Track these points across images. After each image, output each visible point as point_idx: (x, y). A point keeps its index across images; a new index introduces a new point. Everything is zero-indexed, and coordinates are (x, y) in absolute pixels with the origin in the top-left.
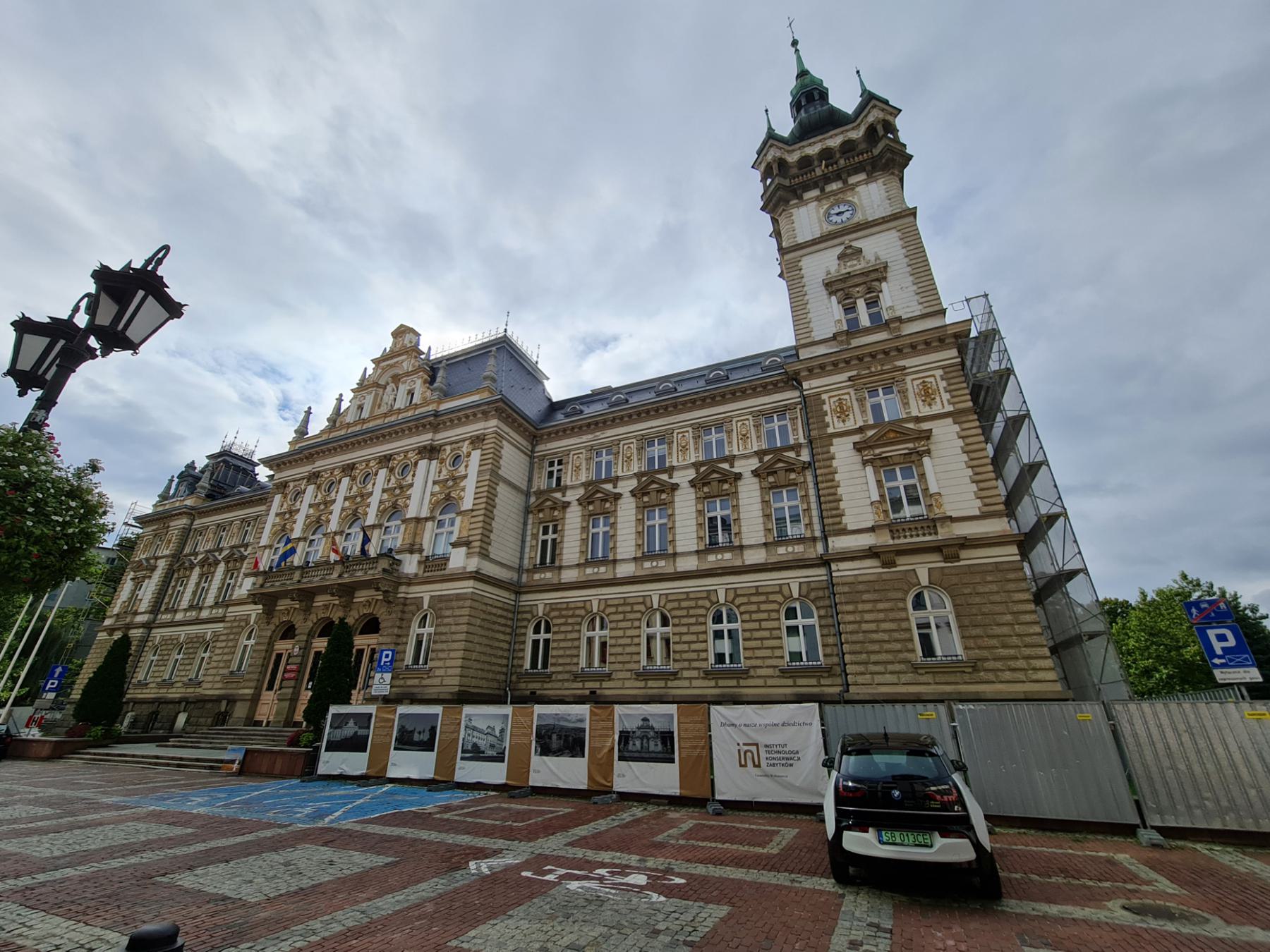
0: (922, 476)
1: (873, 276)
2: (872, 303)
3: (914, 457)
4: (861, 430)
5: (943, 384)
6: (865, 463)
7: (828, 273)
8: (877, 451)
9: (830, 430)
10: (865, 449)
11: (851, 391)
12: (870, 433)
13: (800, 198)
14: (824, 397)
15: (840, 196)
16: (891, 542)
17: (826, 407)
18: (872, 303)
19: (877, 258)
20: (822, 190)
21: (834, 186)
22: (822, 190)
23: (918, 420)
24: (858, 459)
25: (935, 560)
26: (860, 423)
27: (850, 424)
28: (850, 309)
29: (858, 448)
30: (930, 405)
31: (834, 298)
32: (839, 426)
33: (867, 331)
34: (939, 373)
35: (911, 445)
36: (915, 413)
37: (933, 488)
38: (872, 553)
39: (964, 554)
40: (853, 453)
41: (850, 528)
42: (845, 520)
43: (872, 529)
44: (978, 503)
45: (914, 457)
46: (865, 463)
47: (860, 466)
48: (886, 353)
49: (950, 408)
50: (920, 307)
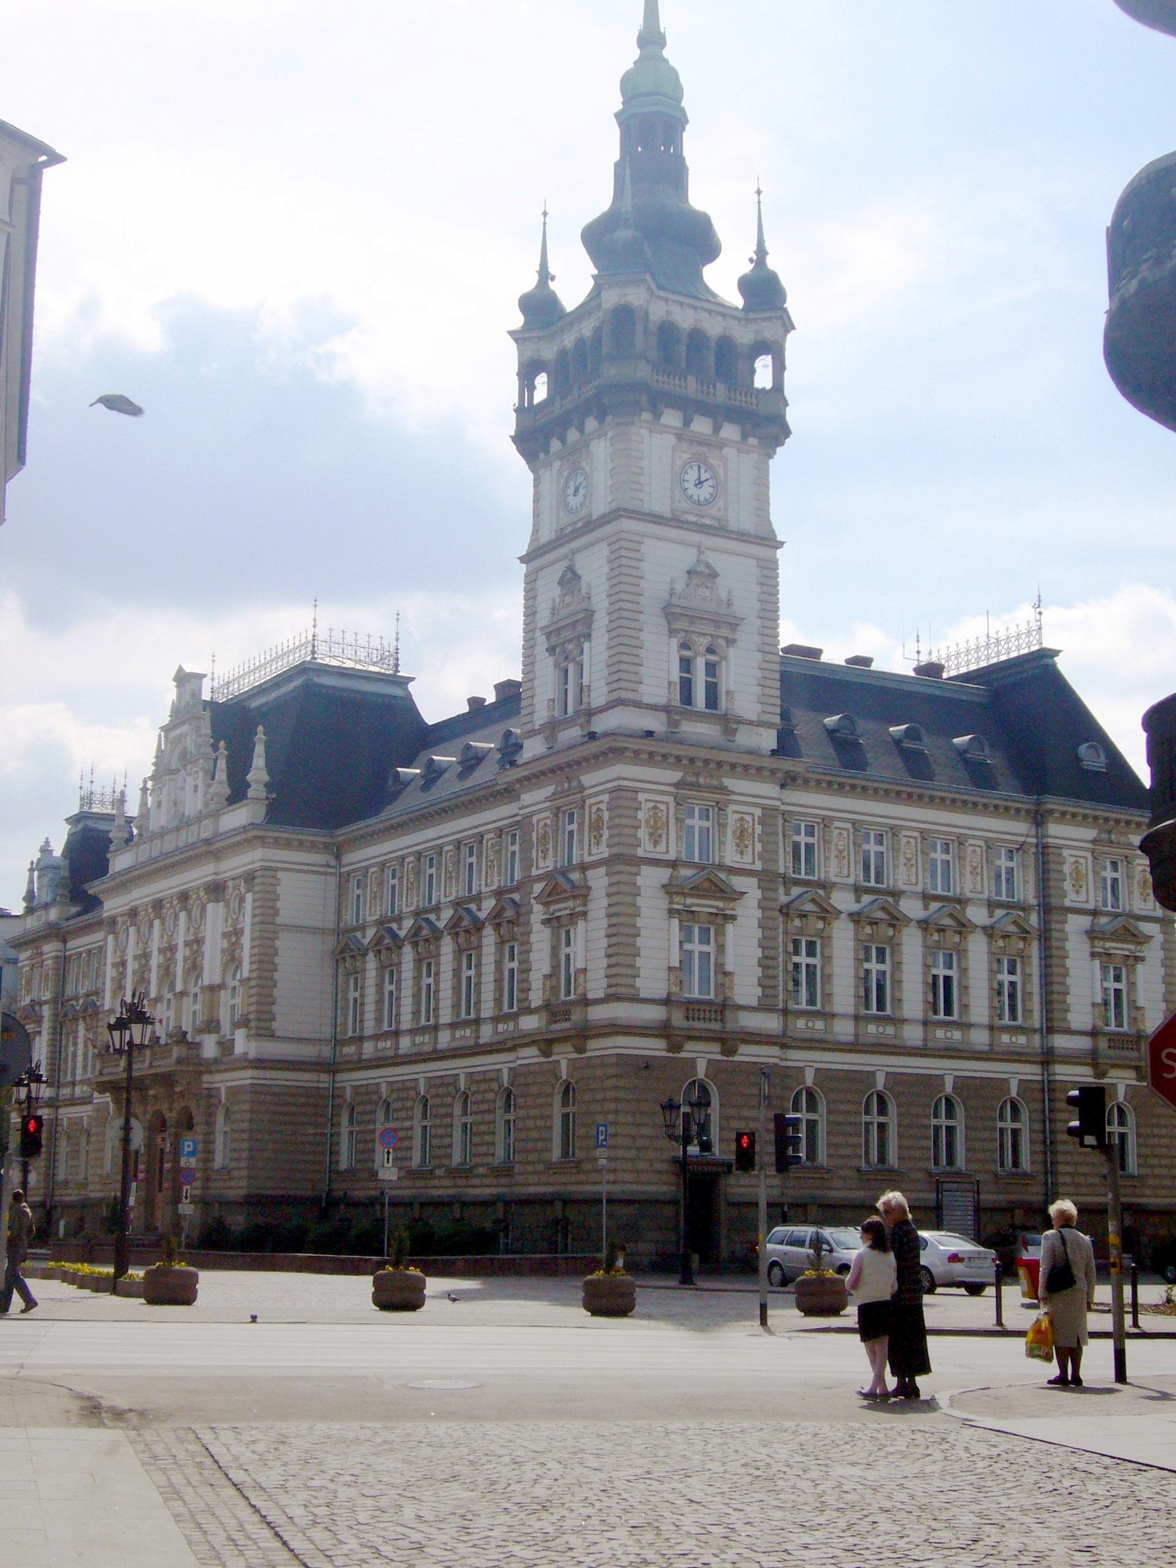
0: (721, 948)
1: (725, 631)
2: (711, 668)
3: (719, 920)
4: (674, 864)
5: (759, 829)
6: (672, 912)
8: (689, 901)
9: (640, 852)
10: (677, 893)
11: (670, 800)
12: (685, 872)
13: (657, 416)
14: (642, 797)
15: (705, 449)
16: (685, 1024)
17: (641, 815)
19: (729, 604)
20: (687, 422)
21: (702, 426)
23: (732, 871)
24: (663, 903)
25: (713, 1051)
26: (672, 856)
27: (659, 852)
28: (686, 664)
29: (670, 889)
30: (742, 853)
34: (758, 812)
35: (720, 904)
36: (728, 862)
37: (729, 967)
39: (744, 1049)
40: (661, 893)
41: (643, 994)
42: (639, 982)
43: (667, 1002)
44: (758, 991)
45: (719, 920)
46: (672, 912)
47: (665, 915)
48: (720, 764)
49: (758, 866)
50: (758, 707)
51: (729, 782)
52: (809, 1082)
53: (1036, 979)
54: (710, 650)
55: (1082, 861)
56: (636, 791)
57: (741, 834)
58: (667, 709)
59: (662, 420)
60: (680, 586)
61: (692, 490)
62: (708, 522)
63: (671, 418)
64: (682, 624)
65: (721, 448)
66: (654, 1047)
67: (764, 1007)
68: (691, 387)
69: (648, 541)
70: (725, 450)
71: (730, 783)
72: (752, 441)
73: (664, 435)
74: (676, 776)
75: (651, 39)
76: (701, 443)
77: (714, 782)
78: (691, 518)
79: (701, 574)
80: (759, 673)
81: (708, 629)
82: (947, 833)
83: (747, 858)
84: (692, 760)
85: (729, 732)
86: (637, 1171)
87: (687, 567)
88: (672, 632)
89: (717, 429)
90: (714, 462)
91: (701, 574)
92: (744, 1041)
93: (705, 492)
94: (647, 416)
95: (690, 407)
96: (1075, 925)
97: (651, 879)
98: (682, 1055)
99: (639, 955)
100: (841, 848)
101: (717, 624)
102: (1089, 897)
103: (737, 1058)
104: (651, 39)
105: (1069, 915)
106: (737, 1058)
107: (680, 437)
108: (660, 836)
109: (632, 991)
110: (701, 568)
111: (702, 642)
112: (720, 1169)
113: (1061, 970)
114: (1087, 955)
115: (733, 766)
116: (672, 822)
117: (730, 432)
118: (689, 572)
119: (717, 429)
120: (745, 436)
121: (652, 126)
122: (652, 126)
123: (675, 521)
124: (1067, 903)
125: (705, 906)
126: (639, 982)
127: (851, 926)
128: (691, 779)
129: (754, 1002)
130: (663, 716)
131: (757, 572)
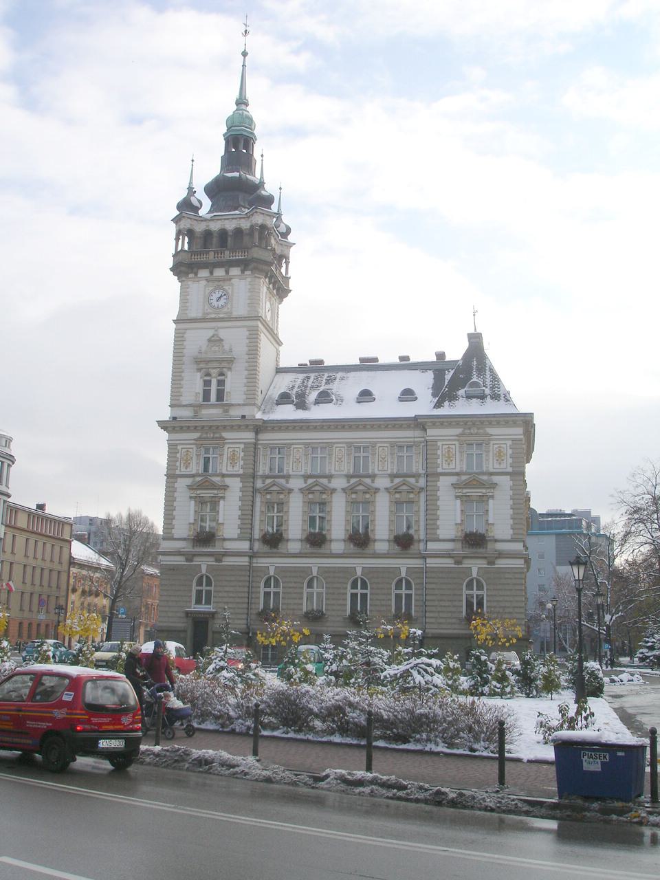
4: (193, 476)
5: (242, 454)
7: (200, 352)
8: (198, 492)
13: (196, 274)
14: (179, 447)
15: (221, 283)
18: (221, 383)
19: (231, 351)
20: (211, 273)
21: (220, 272)
22: (211, 273)
23: (224, 476)
24: (188, 493)
25: (211, 561)
29: (190, 487)
31: (199, 375)
32: (183, 471)
33: (213, 406)
38: (179, 553)
41: (175, 537)
42: (173, 531)
46: (191, 497)
48: (218, 427)
50: (245, 397)
51: (225, 435)
52: (272, 573)
53: (422, 514)
54: (222, 374)
55: (453, 446)
56: (176, 445)
57: (233, 459)
58: (191, 405)
59: (199, 276)
60: (203, 349)
61: (214, 303)
62: (222, 316)
63: (204, 273)
64: (202, 365)
65: (230, 280)
66: (180, 561)
67: (239, 539)
68: (211, 257)
69: (188, 331)
70: (233, 281)
71: (225, 435)
72: (248, 273)
73: (201, 282)
74: (196, 435)
75: (242, 102)
76: (219, 280)
77: (217, 435)
78: (213, 316)
79: (215, 341)
80: (245, 381)
81: (218, 365)
82: (323, 443)
83: (236, 469)
84: (203, 427)
85: (226, 411)
86: (169, 617)
87: (208, 338)
88: (199, 370)
89: (227, 272)
90: (227, 288)
91: (215, 341)
92: (223, 555)
93: (222, 302)
94: (191, 276)
95: (211, 266)
96: (444, 483)
97: (182, 483)
98: (194, 563)
99: (174, 519)
100: (298, 457)
101: (220, 361)
102: (458, 465)
103: (223, 563)
104: (242, 102)
105: (441, 477)
106: (223, 563)
107: (208, 281)
108: (189, 463)
109: (170, 535)
110: (215, 338)
111: (214, 372)
112: (208, 616)
113: (433, 507)
114: (454, 497)
115: (225, 427)
116: (457, 453)
117: (235, 271)
118: (209, 340)
119: (227, 272)
120: (243, 272)
121: (239, 143)
122: (239, 143)
123: (203, 320)
124: (440, 470)
125: (207, 494)
126: (173, 531)
127: (301, 495)
128: (204, 436)
129: (236, 537)
130: (192, 408)
131: (247, 333)
